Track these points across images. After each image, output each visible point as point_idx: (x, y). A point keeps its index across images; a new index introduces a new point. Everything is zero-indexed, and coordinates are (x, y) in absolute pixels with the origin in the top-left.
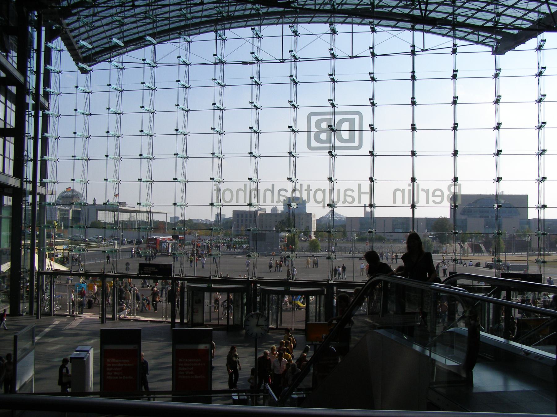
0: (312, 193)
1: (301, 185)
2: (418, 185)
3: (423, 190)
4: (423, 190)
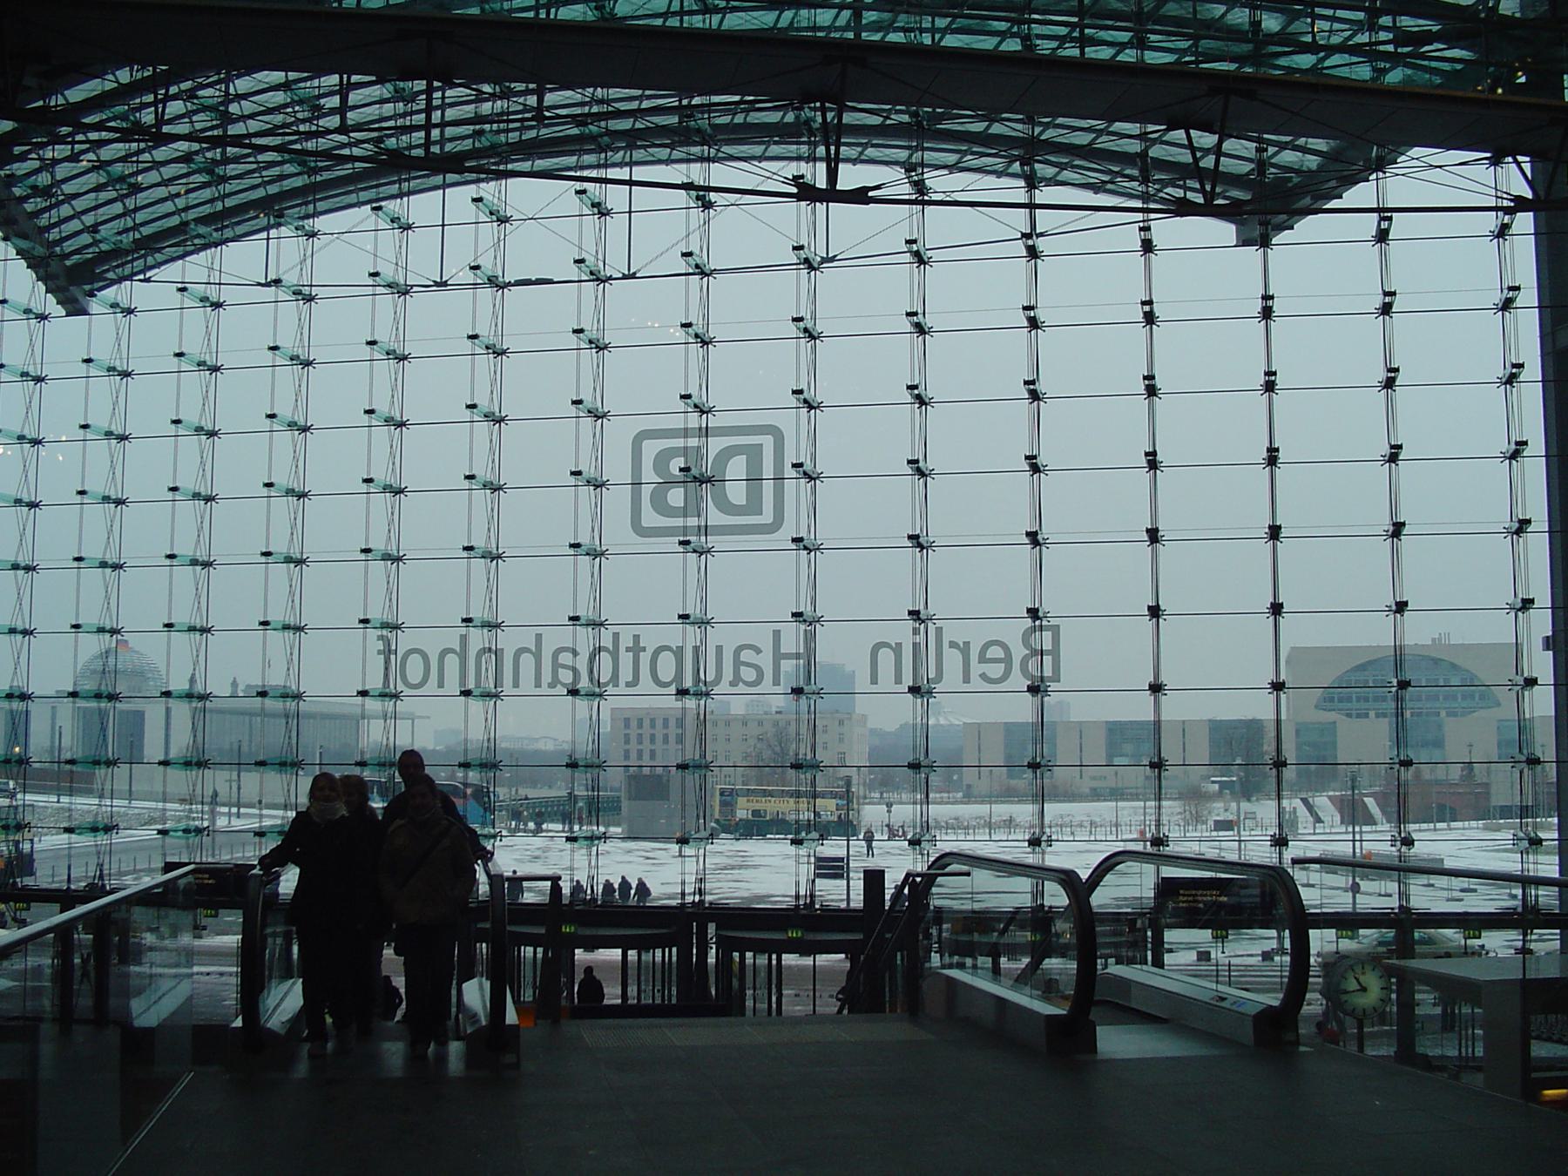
0: (645, 658)
1: (616, 636)
2: (939, 631)
3: (953, 645)
4: (953, 645)
